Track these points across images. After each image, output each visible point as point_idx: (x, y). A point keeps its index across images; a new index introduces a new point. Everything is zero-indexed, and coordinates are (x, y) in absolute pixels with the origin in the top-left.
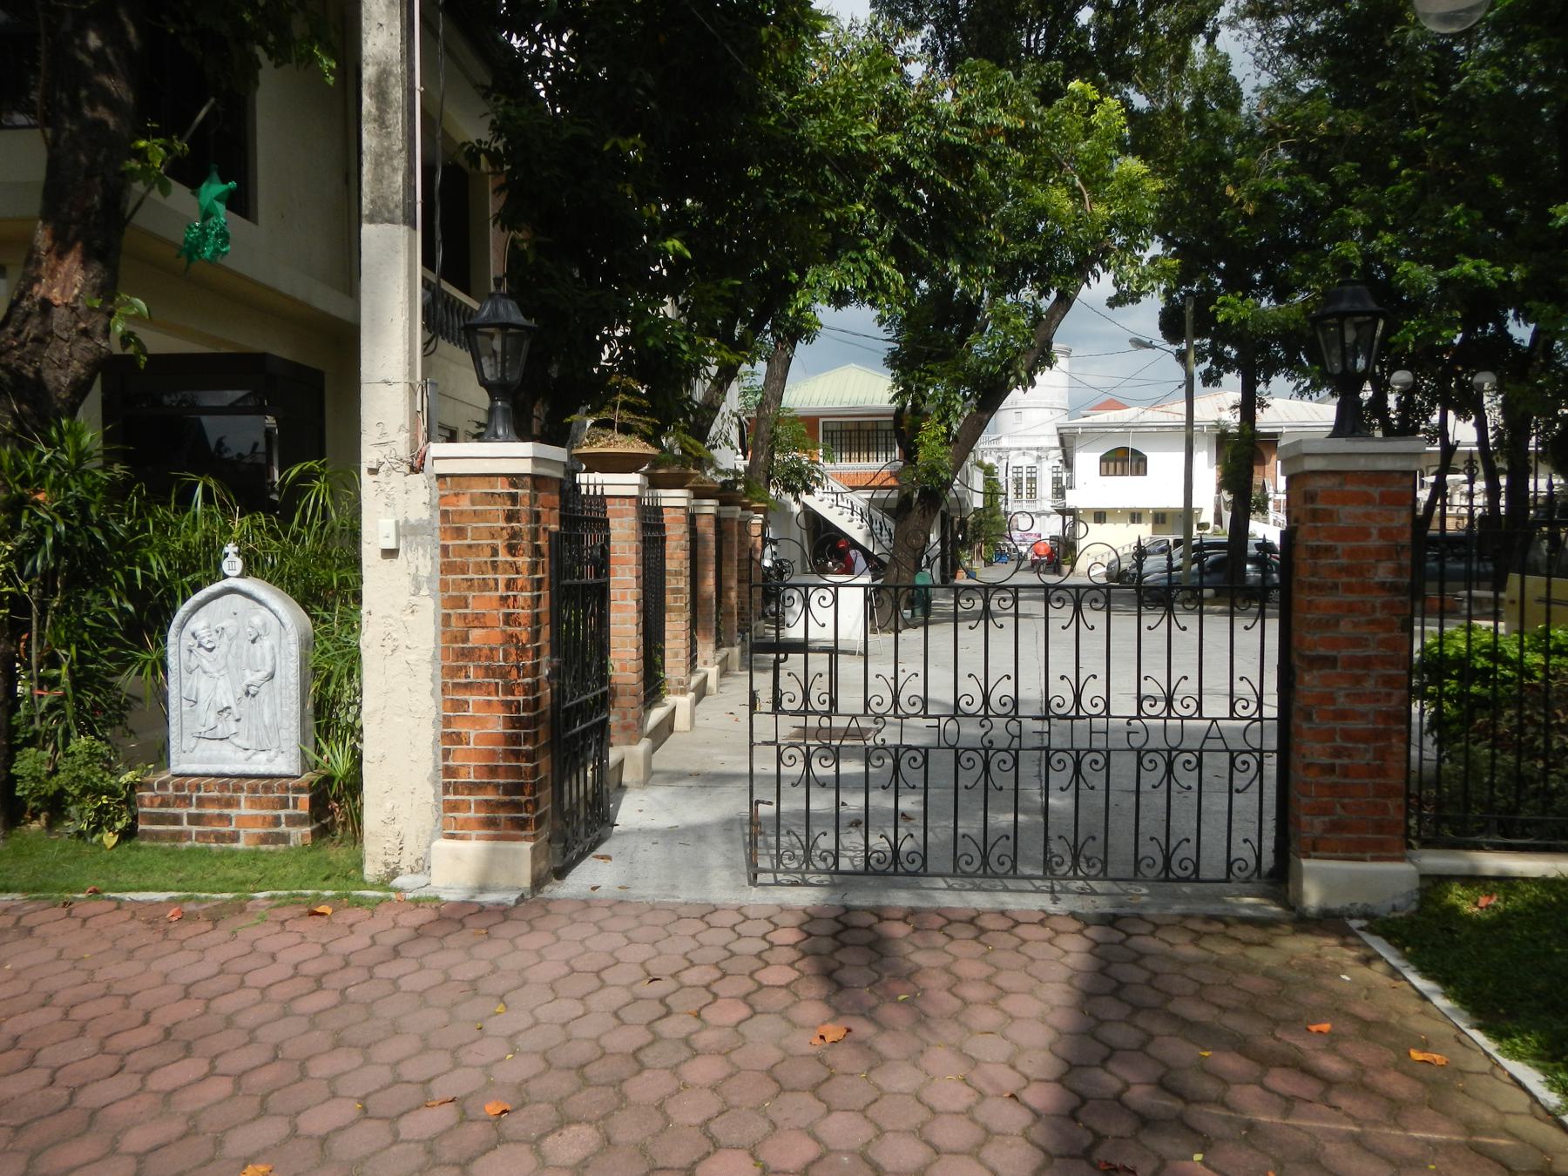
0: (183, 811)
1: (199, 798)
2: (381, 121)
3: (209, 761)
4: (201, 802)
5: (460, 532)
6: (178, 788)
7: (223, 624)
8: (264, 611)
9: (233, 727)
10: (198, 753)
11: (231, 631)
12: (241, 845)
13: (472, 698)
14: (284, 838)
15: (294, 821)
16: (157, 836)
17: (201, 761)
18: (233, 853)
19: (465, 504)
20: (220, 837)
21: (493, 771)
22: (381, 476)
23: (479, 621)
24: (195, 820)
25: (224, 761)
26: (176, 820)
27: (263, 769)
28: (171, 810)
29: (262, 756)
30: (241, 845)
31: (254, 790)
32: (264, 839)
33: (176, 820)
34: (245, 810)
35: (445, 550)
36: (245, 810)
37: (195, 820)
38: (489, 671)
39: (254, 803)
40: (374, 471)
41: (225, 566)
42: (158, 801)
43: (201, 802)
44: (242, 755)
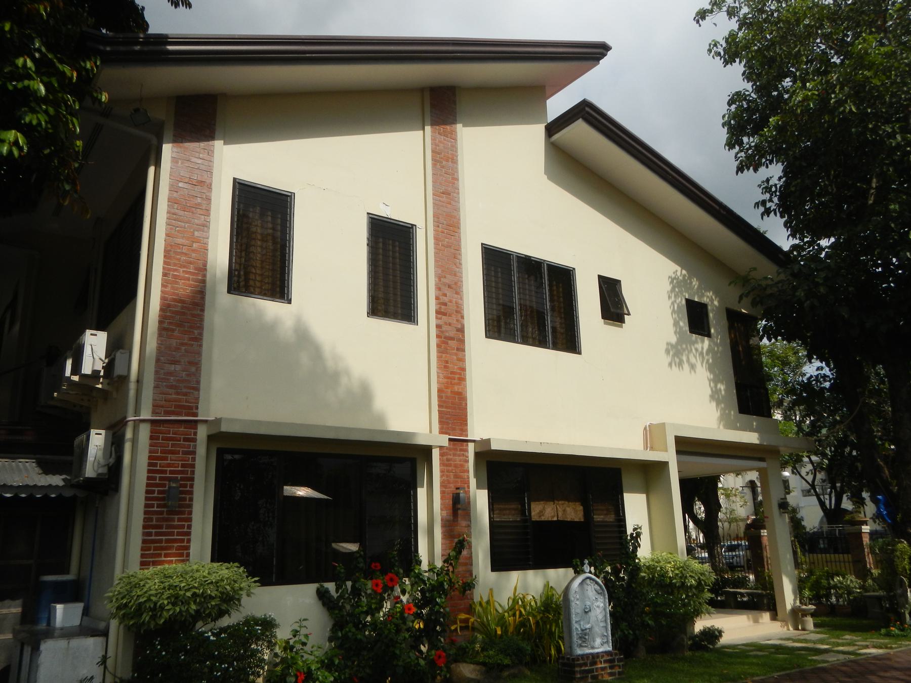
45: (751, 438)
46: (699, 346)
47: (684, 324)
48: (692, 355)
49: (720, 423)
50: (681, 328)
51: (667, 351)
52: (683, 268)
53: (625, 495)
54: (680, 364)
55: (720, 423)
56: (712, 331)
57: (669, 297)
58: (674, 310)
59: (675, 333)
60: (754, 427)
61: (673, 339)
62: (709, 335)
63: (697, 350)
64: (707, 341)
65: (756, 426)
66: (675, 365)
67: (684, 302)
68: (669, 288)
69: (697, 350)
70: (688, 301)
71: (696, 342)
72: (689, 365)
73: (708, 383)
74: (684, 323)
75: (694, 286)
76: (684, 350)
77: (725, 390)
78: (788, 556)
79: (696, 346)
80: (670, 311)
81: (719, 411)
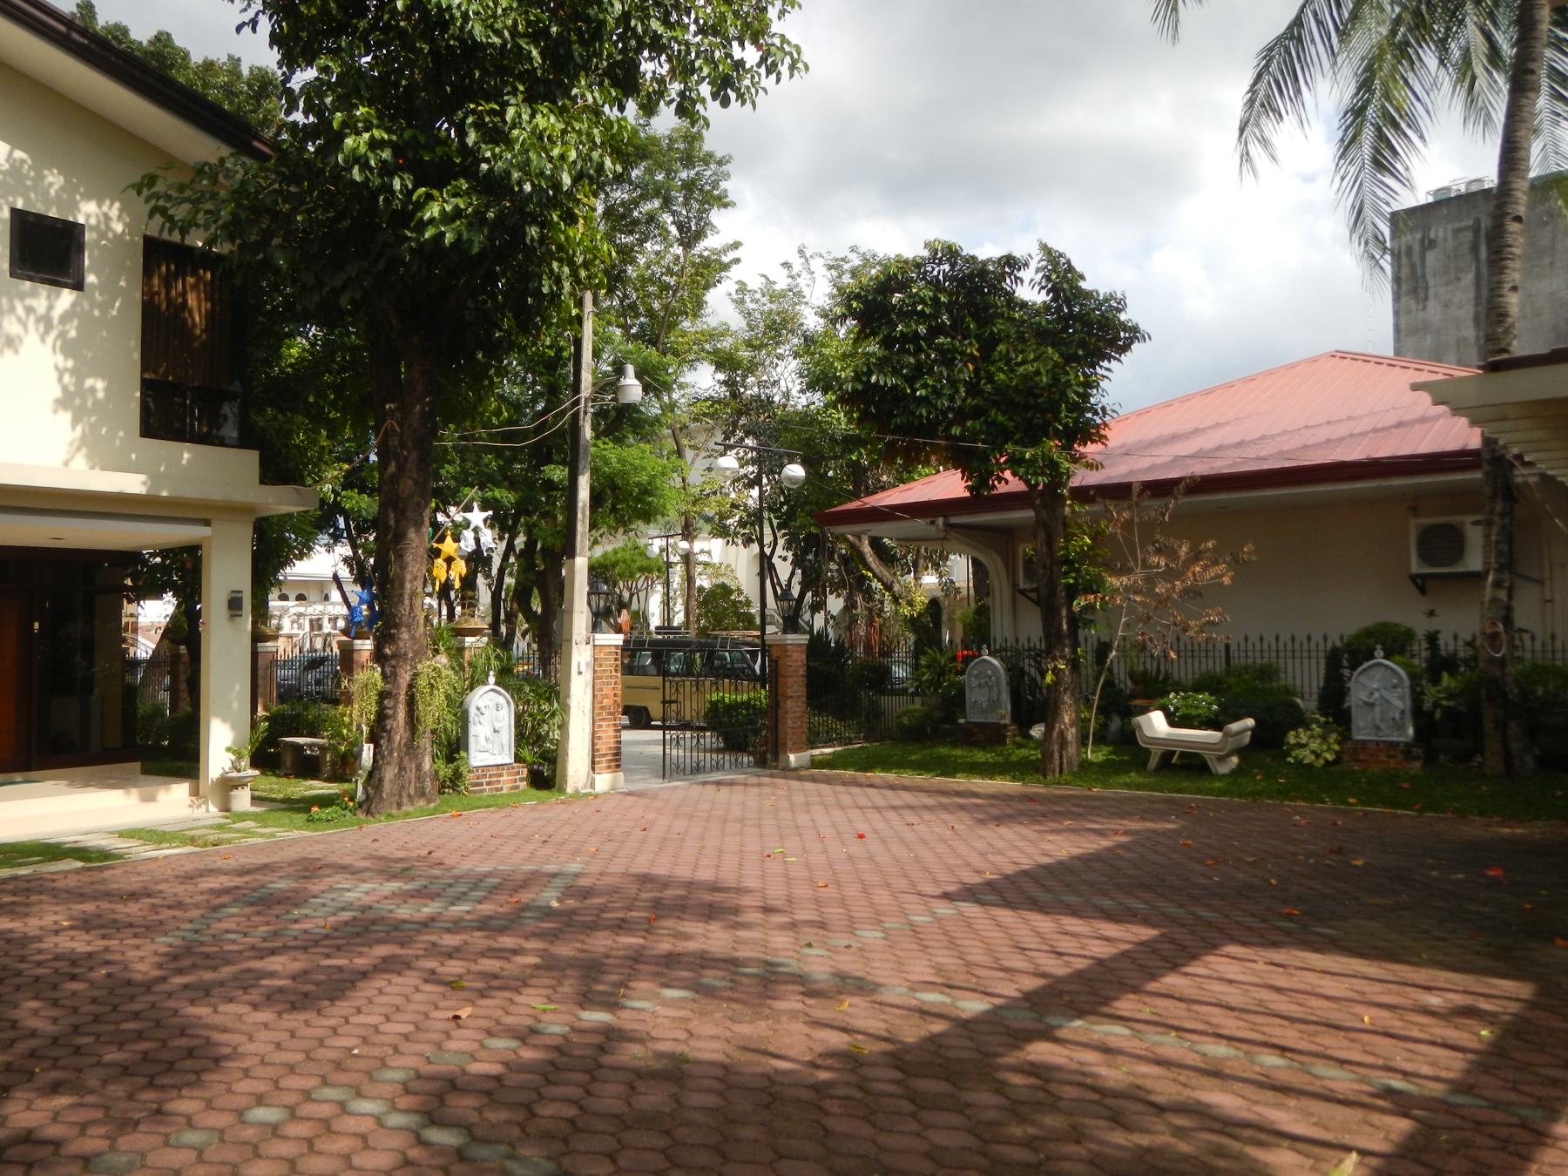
0: (484, 781)
2: (583, 522)
4: (491, 776)
5: (601, 665)
12: (505, 791)
13: (604, 723)
14: (517, 787)
15: (521, 780)
16: (475, 792)
18: (502, 795)
19: (602, 656)
20: (497, 790)
21: (610, 749)
23: (606, 696)
24: (489, 783)
26: (482, 784)
30: (505, 791)
32: (512, 788)
33: (482, 784)
35: (595, 672)
36: (505, 778)
37: (489, 783)
38: (610, 714)
39: (509, 774)
43: (491, 776)
45: (133, 484)
46: (40, 304)
48: (13, 319)
49: (78, 449)
52: (15, 145)
55: (78, 449)
56: (91, 279)
60: (184, 462)
62: (78, 286)
63: (30, 310)
64: (66, 298)
65: (188, 460)
69: (30, 310)
70: (14, 211)
71: (34, 294)
73: (54, 375)
75: (51, 184)
77: (106, 390)
78: (237, 687)
79: (29, 302)
81: (79, 429)
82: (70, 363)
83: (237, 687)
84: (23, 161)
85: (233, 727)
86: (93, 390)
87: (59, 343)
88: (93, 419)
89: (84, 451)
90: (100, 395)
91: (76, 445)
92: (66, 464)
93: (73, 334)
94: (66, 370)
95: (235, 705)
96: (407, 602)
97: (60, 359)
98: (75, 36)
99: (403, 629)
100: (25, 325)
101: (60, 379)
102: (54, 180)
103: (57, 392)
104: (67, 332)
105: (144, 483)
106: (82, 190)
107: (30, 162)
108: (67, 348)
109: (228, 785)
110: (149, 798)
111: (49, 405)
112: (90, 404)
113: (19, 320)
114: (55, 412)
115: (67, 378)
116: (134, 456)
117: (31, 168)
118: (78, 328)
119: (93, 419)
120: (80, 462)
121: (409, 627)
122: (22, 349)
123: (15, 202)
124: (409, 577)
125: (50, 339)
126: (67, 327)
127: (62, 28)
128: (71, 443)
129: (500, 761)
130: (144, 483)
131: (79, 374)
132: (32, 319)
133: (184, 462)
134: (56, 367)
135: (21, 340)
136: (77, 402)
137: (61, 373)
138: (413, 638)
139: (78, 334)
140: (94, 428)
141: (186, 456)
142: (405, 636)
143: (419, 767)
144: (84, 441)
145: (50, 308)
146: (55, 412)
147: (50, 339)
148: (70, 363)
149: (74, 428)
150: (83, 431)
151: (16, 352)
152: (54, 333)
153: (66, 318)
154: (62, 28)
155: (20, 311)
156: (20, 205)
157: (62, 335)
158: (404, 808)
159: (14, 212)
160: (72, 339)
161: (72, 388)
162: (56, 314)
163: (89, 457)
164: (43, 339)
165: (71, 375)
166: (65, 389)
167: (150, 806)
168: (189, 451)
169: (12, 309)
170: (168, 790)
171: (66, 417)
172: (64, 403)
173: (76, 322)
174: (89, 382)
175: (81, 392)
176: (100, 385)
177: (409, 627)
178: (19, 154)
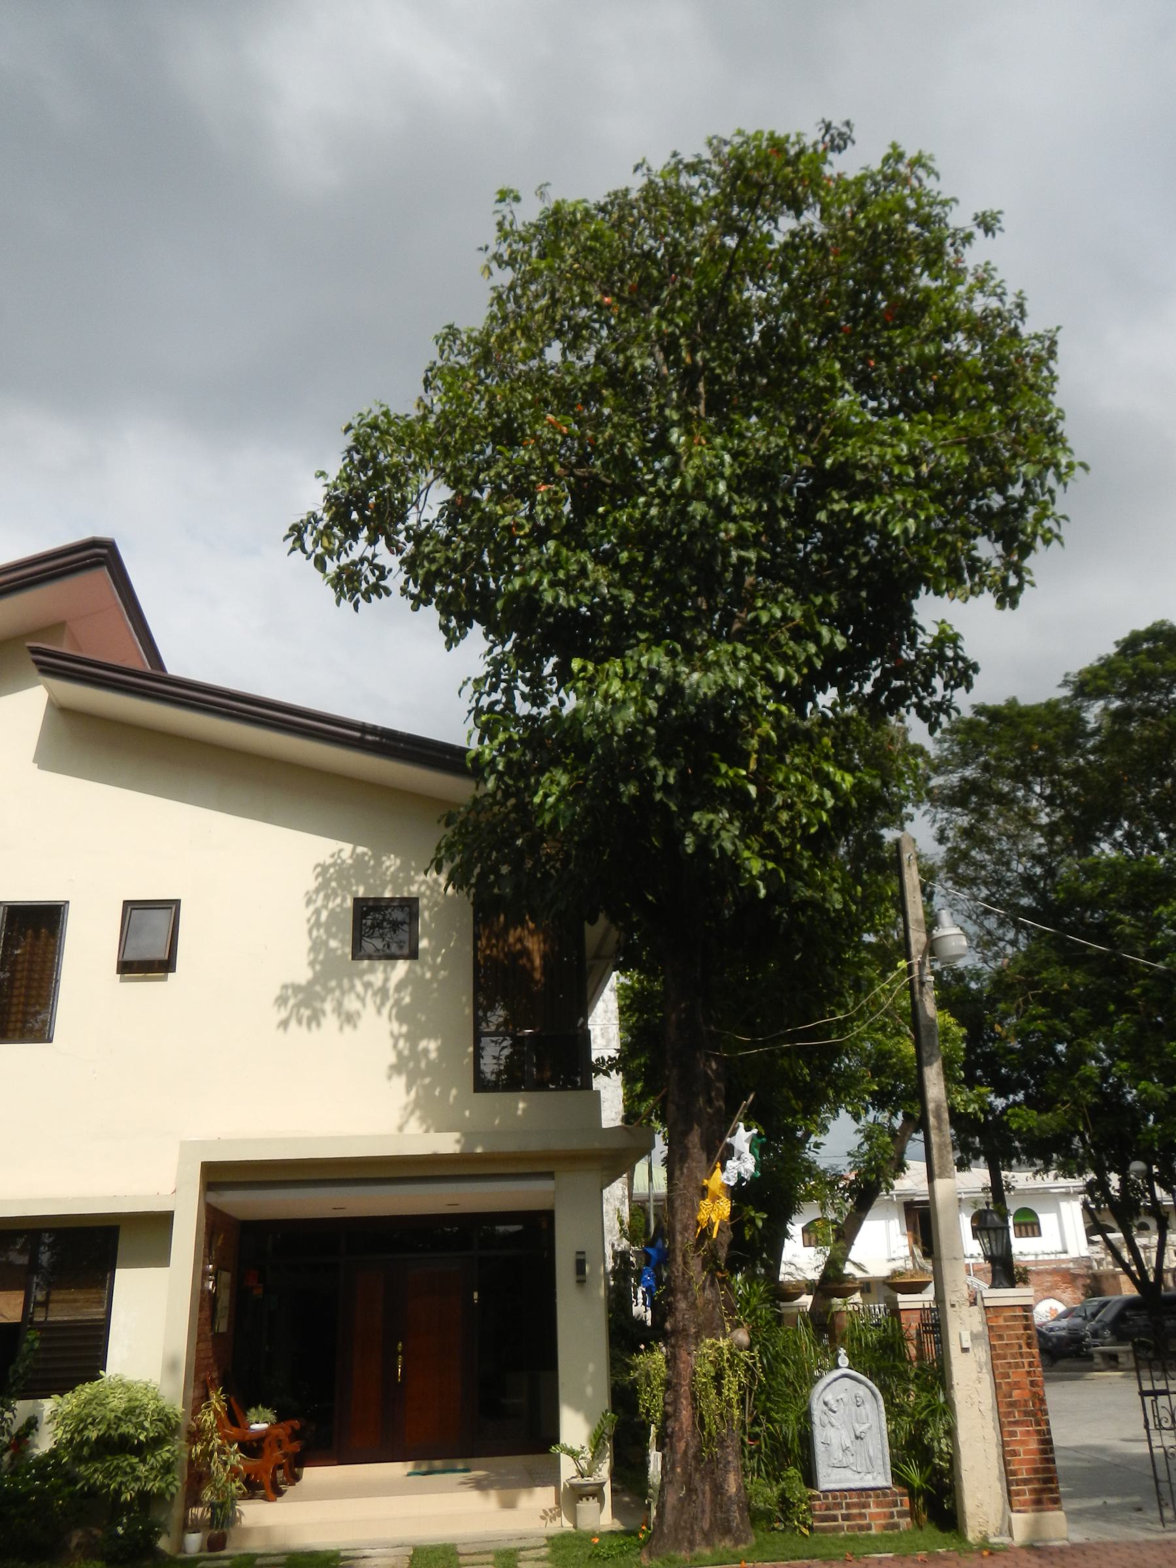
0: (838, 1513)
1: (847, 1504)
3: (840, 1481)
4: (848, 1506)
5: (1000, 1337)
6: (835, 1498)
7: (842, 1396)
8: (862, 1387)
9: (852, 1460)
10: (833, 1477)
11: (845, 1400)
12: (873, 1532)
13: (1018, 1429)
14: (895, 1526)
15: (901, 1514)
16: (824, 1530)
17: (835, 1482)
18: (869, 1537)
19: (1001, 1322)
20: (861, 1528)
21: (1036, 1471)
22: (957, 1308)
23: (1016, 1385)
24: (846, 1518)
25: (848, 1481)
26: (835, 1518)
27: (872, 1484)
28: (832, 1512)
29: (869, 1476)
30: (873, 1532)
31: (877, 1496)
32: (886, 1527)
33: (835, 1518)
34: (873, 1510)
35: (992, 1347)
36: (873, 1510)
37: (846, 1518)
38: (1026, 1413)
39: (878, 1505)
40: (953, 1306)
41: (840, 1361)
42: (824, 1507)
43: (848, 1506)
44: (857, 1476)
46: (377, 978)
47: (341, 945)
48: (353, 996)
49: (412, 1113)
50: (330, 951)
51: (282, 1001)
52: (356, 842)
53: (117, 1271)
54: (315, 1018)
55: (412, 1113)
56: (423, 944)
57: (309, 902)
58: (317, 924)
59: (312, 964)
60: (520, 1112)
61: (303, 975)
62: (413, 955)
63: (368, 985)
64: (401, 968)
65: (524, 1110)
66: (300, 1022)
67: (349, 903)
68: (312, 884)
69: (368, 985)
71: (371, 970)
72: (339, 1015)
73: (390, 1042)
74: (342, 942)
75: (388, 868)
76: (331, 991)
77: (438, 1049)
78: (591, 1367)
79: (367, 978)
80: (306, 927)
81: (413, 1093)
82: (404, 1029)
83: (591, 1367)
84: (364, 854)
85: (588, 1419)
86: (426, 1051)
87: (394, 1011)
88: (427, 1081)
89: (418, 1113)
90: (433, 1055)
91: (410, 1108)
92: (401, 1128)
93: (407, 1000)
94: (401, 1035)
95: (589, 1391)
96: (680, 1259)
97: (395, 1026)
98: (369, 738)
99: (679, 1296)
100: (362, 1000)
101: (395, 1046)
102: (391, 863)
103: (392, 1058)
104: (403, 999)
105: (458, 1141)
106: (413, 864)
107: (370, 853)
108: (403, 1014)
109: (579, 1494)
110: (508, 1504)
111: (384, 1069)
112: (423, 1065)
113: (358, 996)
114: (390, 1078)
115: (401, 1043)
116: (467, 1113)
117: (370, 858)
118: (411, 995)
119: (427, 1081)
120: (414, 1126)
121: (685, 1293)
122: (361, 1024)
123: (357, 892)
124: (678, 1227)
125: (385, 1011)
126: (402, 994)
127: (358, 734)
128: (405, 1108)
129: (869, 1482)
130: (458, 1141)
131: (412, 1038)
132: (370, 993)
133: (520, 1112)
134: (392, 1034)
135: (358, 1014)
136: (411, 1065)
137: (396, 1038)
138: (693, 1306)
139: (413, 999)
140: (428, 1089)
141: (521, 1105)
142: (682, 1305)
143: (718, 1489)
144: (417, 1104)
145: (386, 980)
146: (390, 1078)
147: (385, 1011)
148: (404, 1029)
149: (408, 1091)
150: (417, 1093)
151: (355, 1026)
152: (388, 1005)
153: (400, 987)
154: (358, 734)
155: (359, 988)
156: (361, 892)
157: (397, 1003)
158: (697, 1549)
159: (357, 901)
160: (407, 1006)
161: (406, 1053)
162: (392, 984)
163: (423, 1119)
164: (379, 1012)
165: (406, 1041)
166: (399, 1054)
167: (508, 1513)
168: (524, 1100)
169: (352, 987)
170: (530, 1493)
171: (400, 1082)
172: (396, 1069)
173: (410, 989)
174: (423, 1044)
175: (415, 1055)
176: (431, 1046)
177: (685, 1293)
178: (360, 849)
